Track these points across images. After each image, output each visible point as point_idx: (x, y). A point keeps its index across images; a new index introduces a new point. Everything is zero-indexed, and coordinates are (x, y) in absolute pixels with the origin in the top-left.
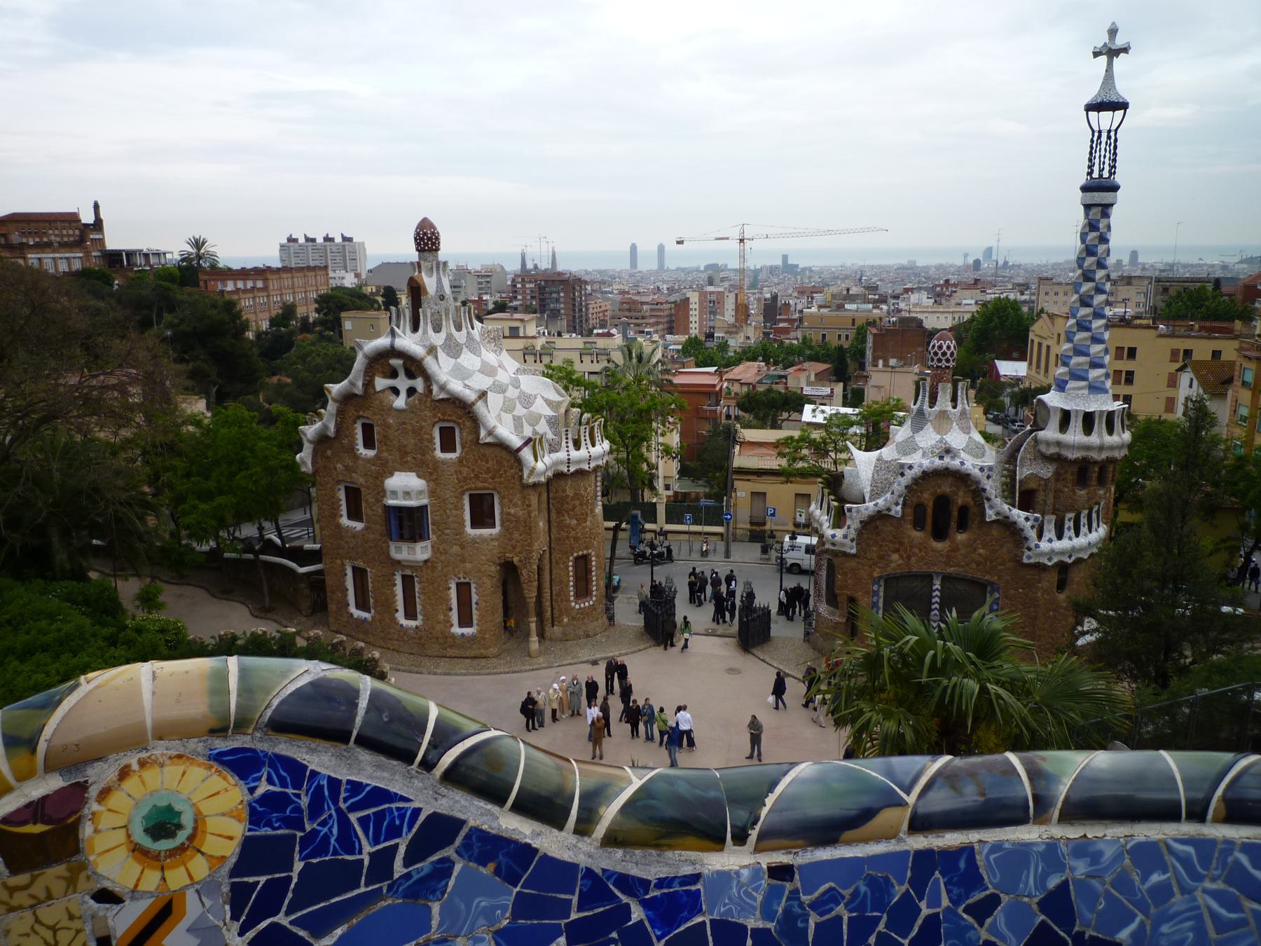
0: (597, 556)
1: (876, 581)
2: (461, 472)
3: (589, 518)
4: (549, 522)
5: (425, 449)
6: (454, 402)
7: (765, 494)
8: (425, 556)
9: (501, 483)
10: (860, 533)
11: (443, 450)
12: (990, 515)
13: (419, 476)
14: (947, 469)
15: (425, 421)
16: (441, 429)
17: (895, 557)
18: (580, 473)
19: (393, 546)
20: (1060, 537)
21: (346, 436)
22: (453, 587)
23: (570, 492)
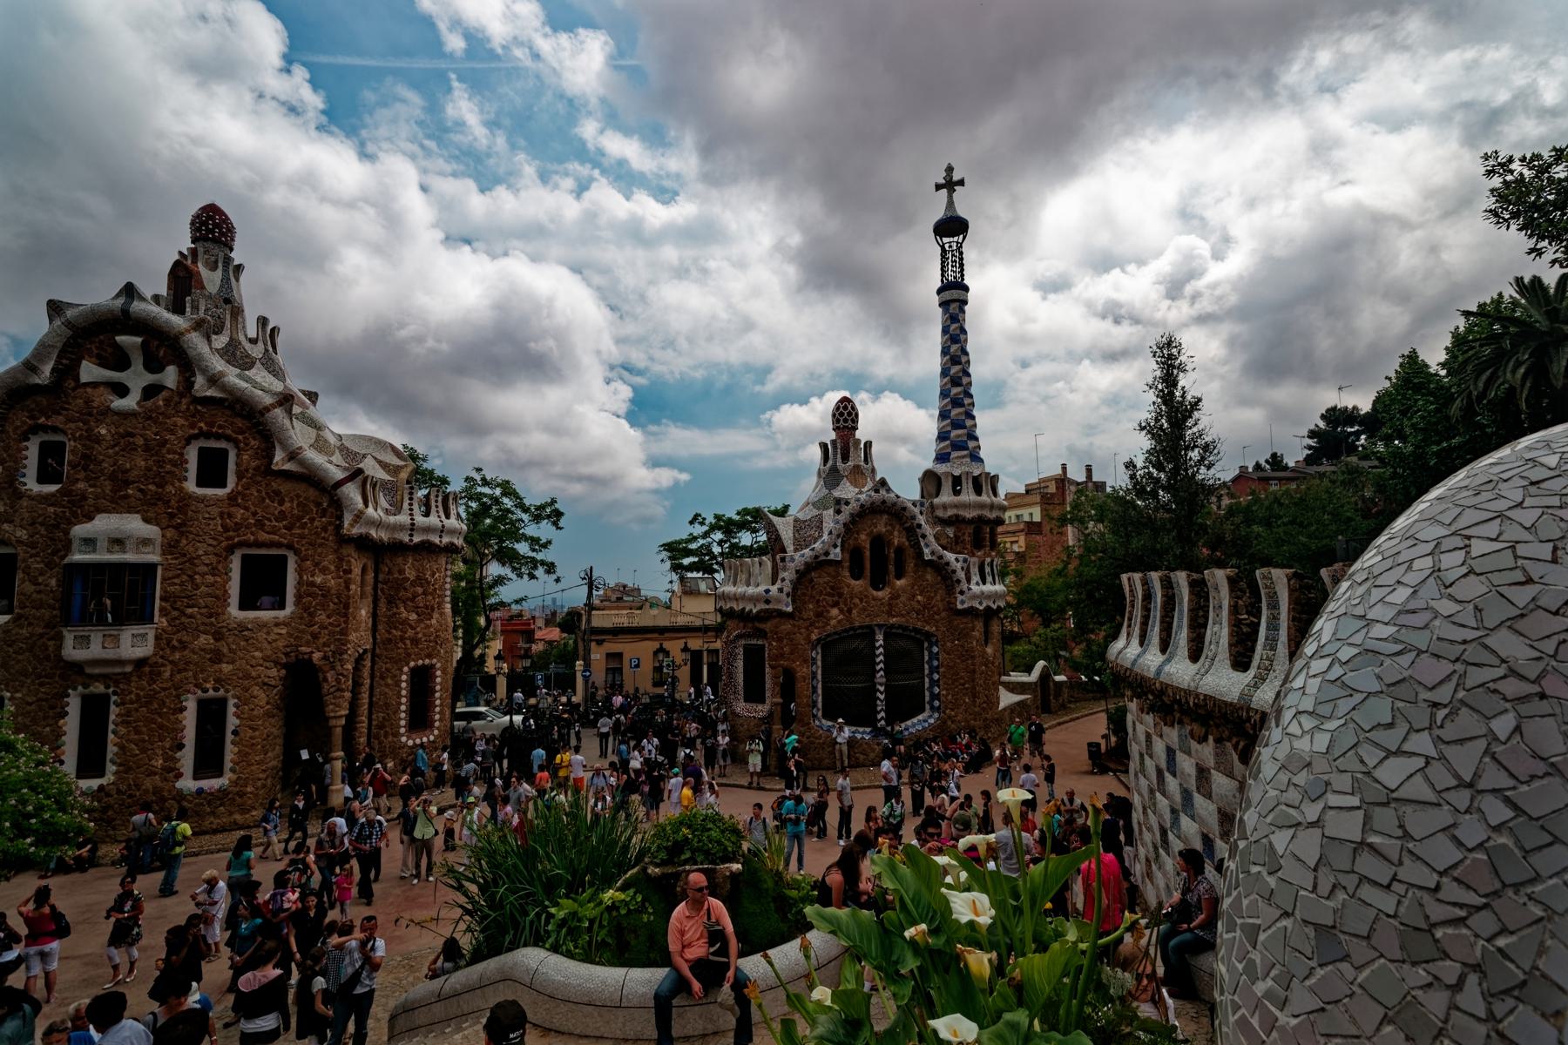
0: (444, 671)
2: (230, 516)
3: (436, 615)
4: (374, 615)
6: (231, 407)
7: (619, 656)
8: (140, 652)
9: (302, 537)
10: (796, 584)
11: (201, 483)
13: (147, 520)
14: (884, 502)
15: (172, 432)
16: (201, 450)
17: (835, 612)
18: (427, 549)
22: (191, 705)
23: (410, 574)
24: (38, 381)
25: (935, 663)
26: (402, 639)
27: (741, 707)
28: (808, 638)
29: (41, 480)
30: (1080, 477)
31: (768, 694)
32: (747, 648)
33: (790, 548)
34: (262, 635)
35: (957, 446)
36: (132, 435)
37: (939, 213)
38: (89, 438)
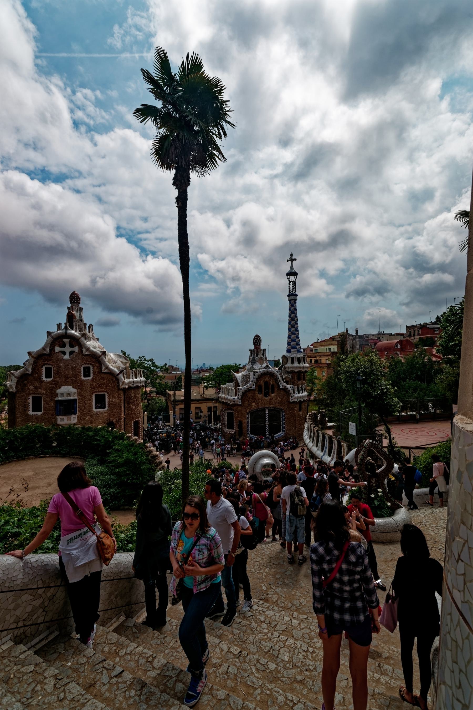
1: (248, 414)
2: (92, 385)
4: (124, 407)
5: (77, 375)
9: (109, 389)
10: (242, 396)
11: (84, 377)
12: (281, 387)
13: (73, 387)
15: (78, 364)
17: (254, 404)
19: (59, 418)
20: (299, 393)
21: (37, 373)
23: (133, 395)
24: (46, 353)
25: (284, 418)
26: (132, 413)
27: (226, 430)
28: (246, 411)
29: (46, 377)
30: (354, 333)
31: (234, 427)
32: (228, 414)
33: (241, 384)
34: (101, 416)
35: (293, 348)
36: (68, 365)
37: (288, 270)
38: (58, 367)
